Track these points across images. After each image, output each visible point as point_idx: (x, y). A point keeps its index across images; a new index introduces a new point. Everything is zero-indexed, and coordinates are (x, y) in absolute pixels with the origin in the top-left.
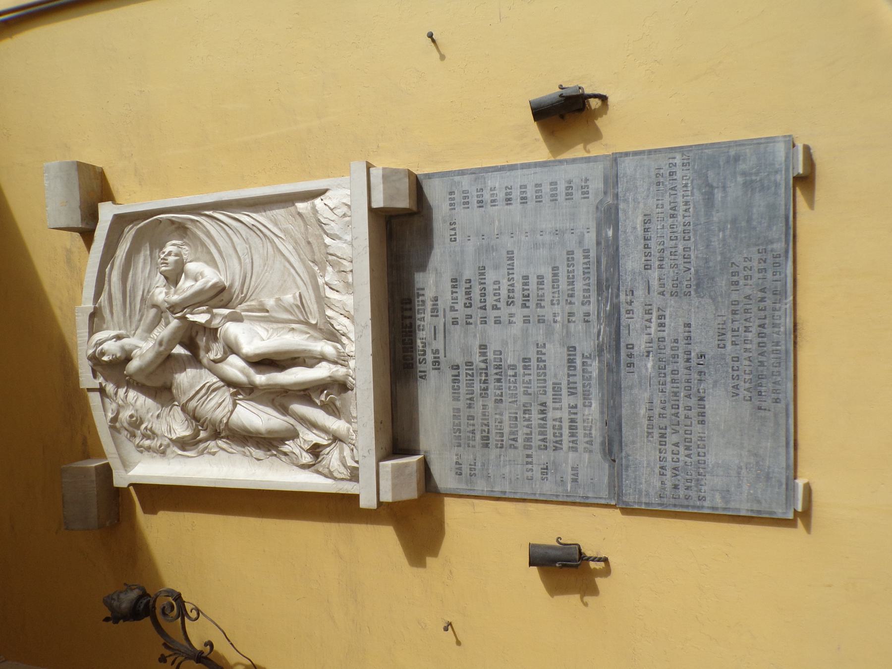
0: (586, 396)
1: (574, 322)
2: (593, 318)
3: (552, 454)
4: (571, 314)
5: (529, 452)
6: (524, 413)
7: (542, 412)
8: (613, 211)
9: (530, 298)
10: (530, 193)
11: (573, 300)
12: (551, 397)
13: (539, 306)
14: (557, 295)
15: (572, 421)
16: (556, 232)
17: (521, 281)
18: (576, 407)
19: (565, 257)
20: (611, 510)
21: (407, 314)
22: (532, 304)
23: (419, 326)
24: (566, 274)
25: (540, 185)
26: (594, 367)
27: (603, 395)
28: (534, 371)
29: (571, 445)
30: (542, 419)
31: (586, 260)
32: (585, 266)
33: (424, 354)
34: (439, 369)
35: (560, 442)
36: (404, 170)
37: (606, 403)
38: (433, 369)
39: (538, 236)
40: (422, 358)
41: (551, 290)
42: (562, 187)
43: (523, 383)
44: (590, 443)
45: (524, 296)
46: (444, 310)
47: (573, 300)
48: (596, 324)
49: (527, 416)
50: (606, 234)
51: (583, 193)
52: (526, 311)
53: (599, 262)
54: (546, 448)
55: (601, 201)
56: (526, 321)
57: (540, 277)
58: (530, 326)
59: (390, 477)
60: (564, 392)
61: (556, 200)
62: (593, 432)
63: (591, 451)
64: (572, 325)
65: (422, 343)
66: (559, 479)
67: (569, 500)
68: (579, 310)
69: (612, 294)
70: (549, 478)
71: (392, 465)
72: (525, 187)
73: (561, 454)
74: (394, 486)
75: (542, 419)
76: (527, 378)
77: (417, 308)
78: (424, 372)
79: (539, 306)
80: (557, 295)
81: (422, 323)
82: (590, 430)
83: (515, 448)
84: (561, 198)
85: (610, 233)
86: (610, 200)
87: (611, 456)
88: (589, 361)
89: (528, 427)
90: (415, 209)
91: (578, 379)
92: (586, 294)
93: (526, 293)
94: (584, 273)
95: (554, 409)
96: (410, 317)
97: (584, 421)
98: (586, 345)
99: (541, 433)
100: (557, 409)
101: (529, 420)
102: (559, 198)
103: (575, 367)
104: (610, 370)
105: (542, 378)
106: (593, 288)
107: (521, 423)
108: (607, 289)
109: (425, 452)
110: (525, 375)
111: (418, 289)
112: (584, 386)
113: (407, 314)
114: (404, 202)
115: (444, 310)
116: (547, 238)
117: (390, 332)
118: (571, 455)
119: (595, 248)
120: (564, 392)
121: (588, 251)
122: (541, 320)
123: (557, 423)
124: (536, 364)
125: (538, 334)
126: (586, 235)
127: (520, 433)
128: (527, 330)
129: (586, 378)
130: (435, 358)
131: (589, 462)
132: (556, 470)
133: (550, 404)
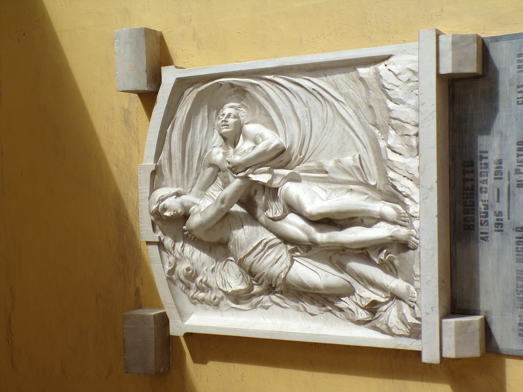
21: (469, 176)
23: (481, 188)
33: (487, 216)
34: (502, 231)
36: (473, 36)
38: (496, 231)
40: (484, 219)
46: (509, 173)
59: (453, 333)
65: (484, 205)
71: (456, 322)
74: (458, 344)
77: (479, 170)
78: (486, 233)
81: (485, 185)
90: (480, 73)
96: (472, 180)
109: (486, 312)
111: (481, 152)
113: (469, 176)
114: (471, 67)
115: (509, 173)
117: (451, 194)
130: (498, 220)
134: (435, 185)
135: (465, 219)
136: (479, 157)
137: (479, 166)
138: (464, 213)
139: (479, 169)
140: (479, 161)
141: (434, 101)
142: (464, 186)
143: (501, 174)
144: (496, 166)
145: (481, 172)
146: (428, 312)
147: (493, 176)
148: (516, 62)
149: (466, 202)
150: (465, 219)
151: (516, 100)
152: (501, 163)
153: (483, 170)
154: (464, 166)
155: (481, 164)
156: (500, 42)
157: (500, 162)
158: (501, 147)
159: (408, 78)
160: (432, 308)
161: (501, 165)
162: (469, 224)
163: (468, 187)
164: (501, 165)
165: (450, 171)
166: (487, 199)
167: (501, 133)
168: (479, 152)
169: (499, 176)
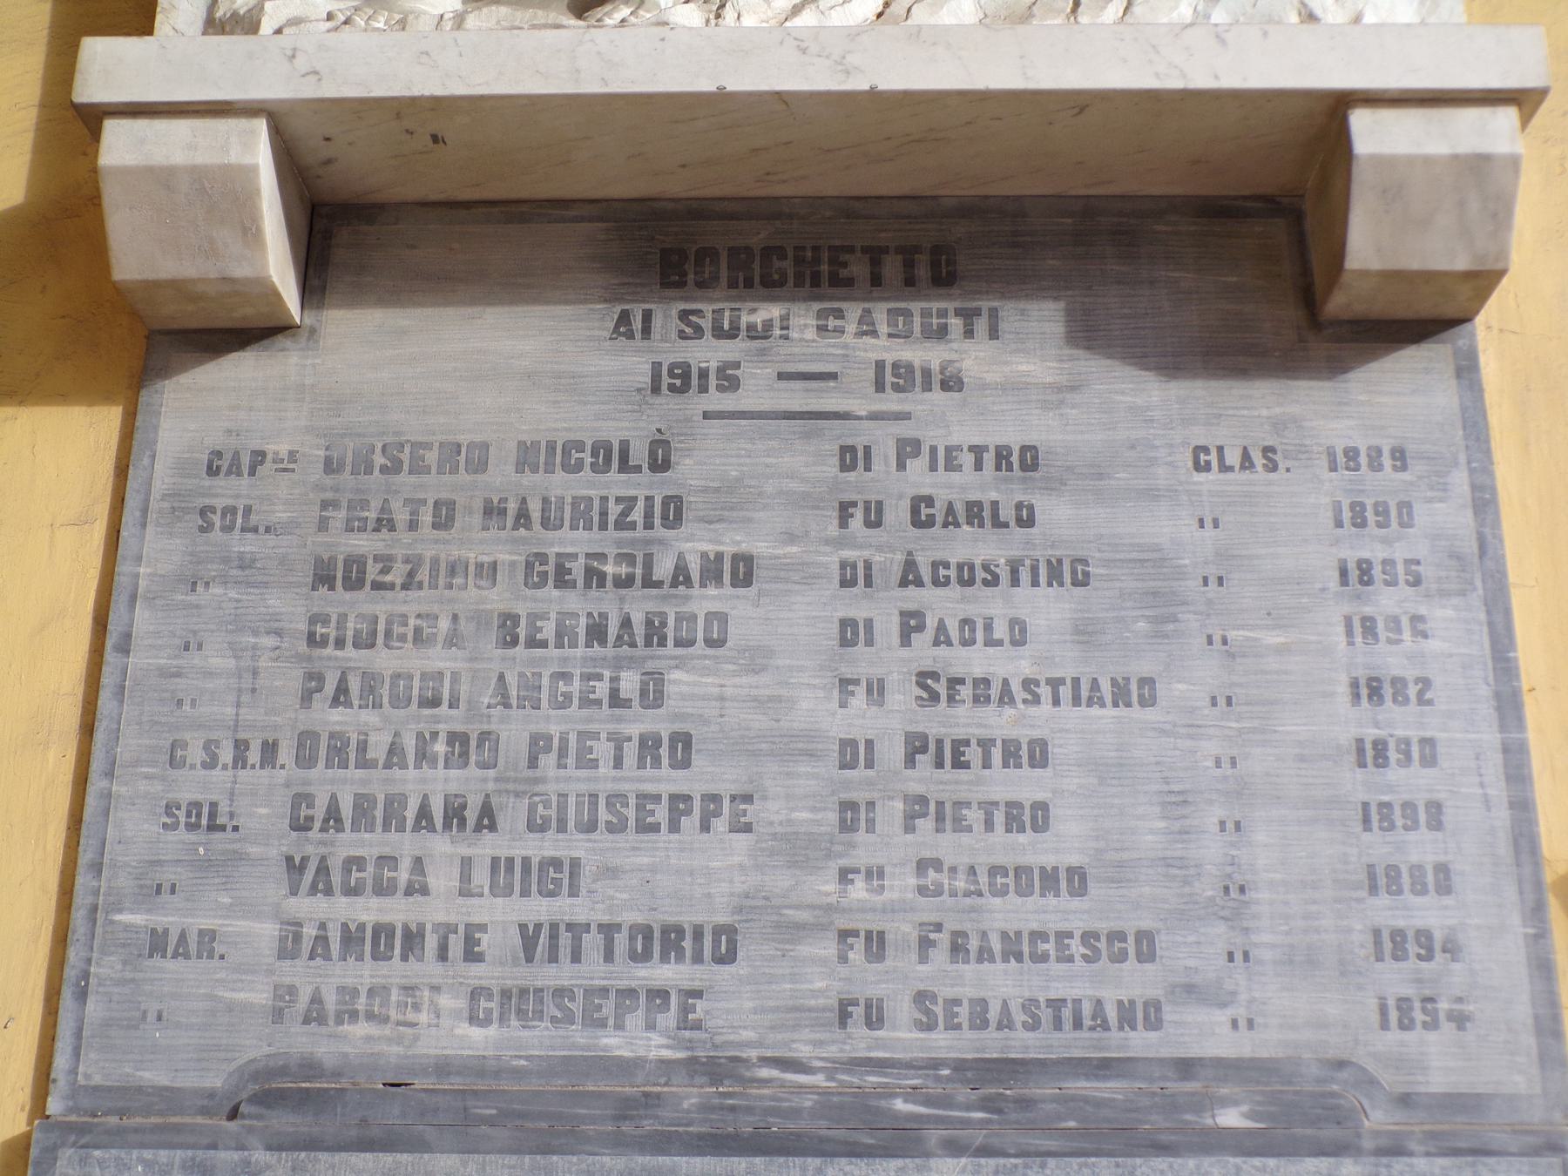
0: (518, 1003)
1: (843, 959)
2: (860, 1041)
3: (275, 852)
4: (876, 944)
5: (286, 755)
6: (452, 738)
7: (455, 814)
8: (1330, 1133)
9: (948, 773)
10: (1406, 782)
11: (940, 955)
12: (518, 852)
13: (917, 807)
14: (961, 884)
15: (413, 939)
16: (1236, 890)
17: (1024, 734)
18: (472, 954)
19: (1131, 925)
20: (24, 1096)
21: (892, 267)
22: (924, 778)
23: (839, 314)
24: (1054, 924)
25: (1436, 824)
26: (642, 1041)
27: (518, 1073)
28: (635, 779)
29: (310, 931)
30: (424, 813)
31: (1112, 1014)
32: (1087, 1009)
33: (719, 333)
34: (656, 389)
35: (322, 885)
36: (1503, 254)
37: (481, 1085)
38: (656, 367)
39: (1217, 812)
40: (706, 324)
41: (983, 861)
42: (1428, 913)
43: (583, 736)
44: (315, 1015)
45: (959, 745)
46: (906, 416)
47: (940, 955)
48: (832, 1051)
49: (440, 748)
50: (1226, 1102)
51: (1404, 1004)
52: (892, 752)
53: (1104, 1067)
54: (300, 826)
55: (1373, 1082)
56: (852, 753)
57: (1039, 817)
58: (829, 767)
59: (201, 158)
60: (539, 909)
61: (1373, 889)
62: (362, 1029)
63: (278, 1015)
64: (827, 948)
65: (768, 325)
66: (167, 875)
67: (79, 916)
68: (893, 981)
69: (966, 1124)
70: (171, 836)
71: (253, 170)
72: (1429, 760)
73: (273, 889)
74: (162, 177)
75: (424, 813)
76: (603, 750)
77: (916, 307)
78: (647, 331)
79: (917, 807)
80: (961, 884)
81: (851, 328)
82: (370, 1016)
83: (306, 698)
84: (1384, 911)
85: (1231, 1118)
86: (1378, 1118)
87: (256, 1099)
88: (668, 1019)
89: (394, 750)
90: (1337, 304)
91: (593, 970)
92: (963, 1012)
93: (973, 754)
94: (1056, 1004)
95: (466, 863)
96: (876, 281)
97: (408, 989)
98: (739, 1008)
99: (363, 806)
100: (466, 877)
101: (423, 756)
102: (1384, 900)
103: (646, 956)
104: (627, 1109)
105: (603, 815)
106: (992, 1043)
107: (411, 724)
108: (986, 1104)
109: (313, 331)
110: (618, 741)
111: (993, 314)
112: (560, 992)
113: (892, 267)
114: (1369, 243)
115: (906, 416)
116: (1210, 850)
117: (816, 202)
118: (268, 931)
119: (1165, 1053)
120: (539, 909)
121: (1154, 1023)
122: (851, 815)
123: (403, 876)
124: (665, 789)
125: (795, 800)
126: (1221, 1017)
127: (369, 717)
128: (811, 754)
129: (595, 1006)
130: (703, 374)
131: (231, 1007)
132: (204, 866)
133: (488, 846)
134: (860, 84)
135: (706, 255)
136: (975, 304)
137: (935, 306)
138: (733, 252)
139: (924, 305)
140: (958, 304)
141: (1231, 80)
142: (850, 250)
143: (897, 388)
144: (935, 366)
145: (907, 314)
146: (297, 62)
147: (889, 358)
148: (1375, 442)
149: (784, 257)
150: (706, 255)
151: (1213, 444)
152: (945, 386)
153: (917, 320)
154: (936, 250)
155: (943, 314)
156: (1454, 382)
157: (951, 383)
158: (1014, 388)
159: (1318, 12)
160: (316, 73)
161: (936, 385)
162: (690, 267)
163: (845, 265)
164: (936, 385)
165: (914, 198)
166: (794, 335)
167: (1073, 388)
168: (995, 304)
169: (889, 378)
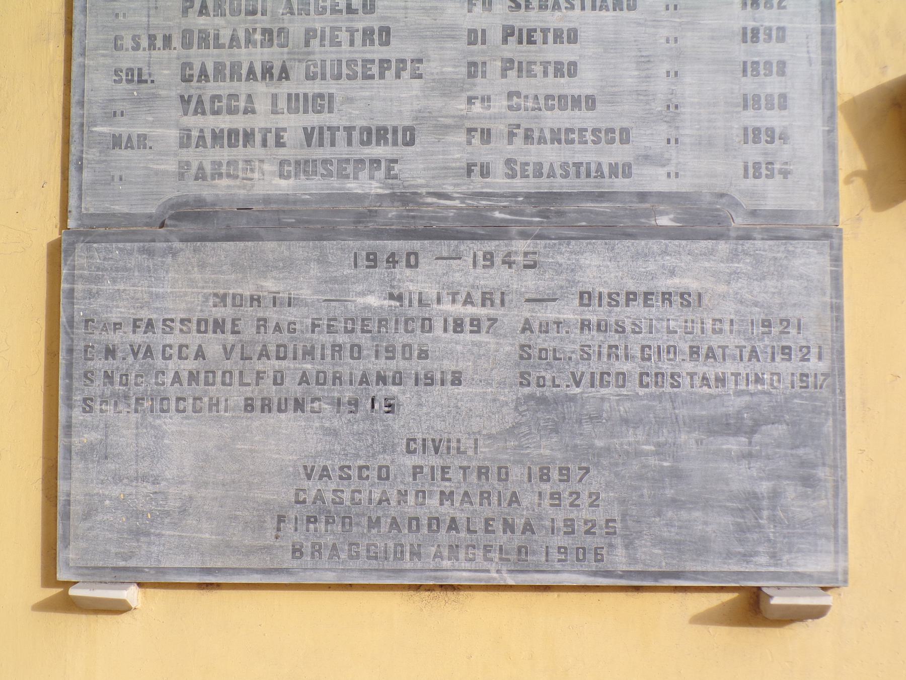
0: (304, 167)
1: (469, 143)
2: (477, 184)
3: (174, 93)
4: (486, 135)
5: (176, 42)
6: (264, 31)
7: (267, 71)
8: (714, 228)
9: (525, 46)
10: (767, 50)
11: (519, 141)
12: (301, 91)
13: (508, 65)
14: (530, 104)
15: (249, 136)
16: (673, 107)
17: (565, 26)
18: (279, 144)
19: (617, 125)
20: (56, 220)
22: (512, 49)
24: (578, 125)
25: (782, 72)
26: (368, 185)
27: (305, 202)
28: (362, 52)
29: (195, 134)
30: (251, 71)
31: (606, 170)
32: (593, 167)
35: (200, 110)
37: (286, 207)
39: (666, 67)
41: (542, 92)
42: (773, 119)
43: (333, 29)
44: (201, 175)
45: (531, 32)
47: (519, 141)
48: (464, 189)
49: (258, 37)
50: (662, 213)
51: (757, 165)
52: (495, 36)
53: (601, 196)
54: (187, 79)
55: (738, 204)
56: (475, 37)
57: (572, 69)
58: (462, 44)
60: (313, 120)
61: (745, 107)
62: (225, 182)
63: (181, 176)
64: (462, 137)
66: (118, 107)
67: (74, 129)
68: (494, 154)
69: (530, 223)
70: (119, 86)
72: (781, 39)
73: (175, 112)
75: (251, 71)
76: (344, 36)
79: (508, 65)
80: (530, 104)
82: (229, 176)
83: (185, 12)
84: (750, 118)
85: (664, 221)
86: (739, 221)
87: (172, 217)
88: (381, 174)
89: (234, 39)
91: (342, 150)
92: (530, 169)
93: (538, 36)
94: (578, 165)
95: (275, 97)
97: (247, 162)
98: (416, 168)
99: (219, 68)
100: (274, 103)
101: (249, 41)
102: (750, 112)
103: (368, 143)
104: (360, 218)
105: (345, 71)
106: (544, 185)
107: (242, 23)
108: (540, 214)
110: (352, 32)
112: (325, 162)
116: (661, 86)
118: (173, 134)
119: (632, 189)
120: (313, 120)
121: (627, 174)
122: (474, 69)
123: (242, 104)
124: (377, 57)
125: (446, 61)
126: (662, 171)
127: (219, 21)
128: (453, 37)
129: (343, 169)
131: (157, 173)
132: (137, 101)
133: (285, 88)
